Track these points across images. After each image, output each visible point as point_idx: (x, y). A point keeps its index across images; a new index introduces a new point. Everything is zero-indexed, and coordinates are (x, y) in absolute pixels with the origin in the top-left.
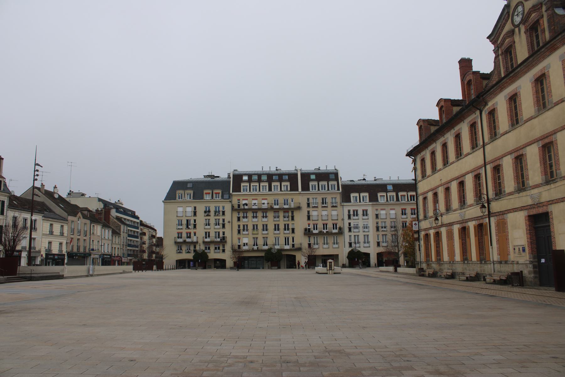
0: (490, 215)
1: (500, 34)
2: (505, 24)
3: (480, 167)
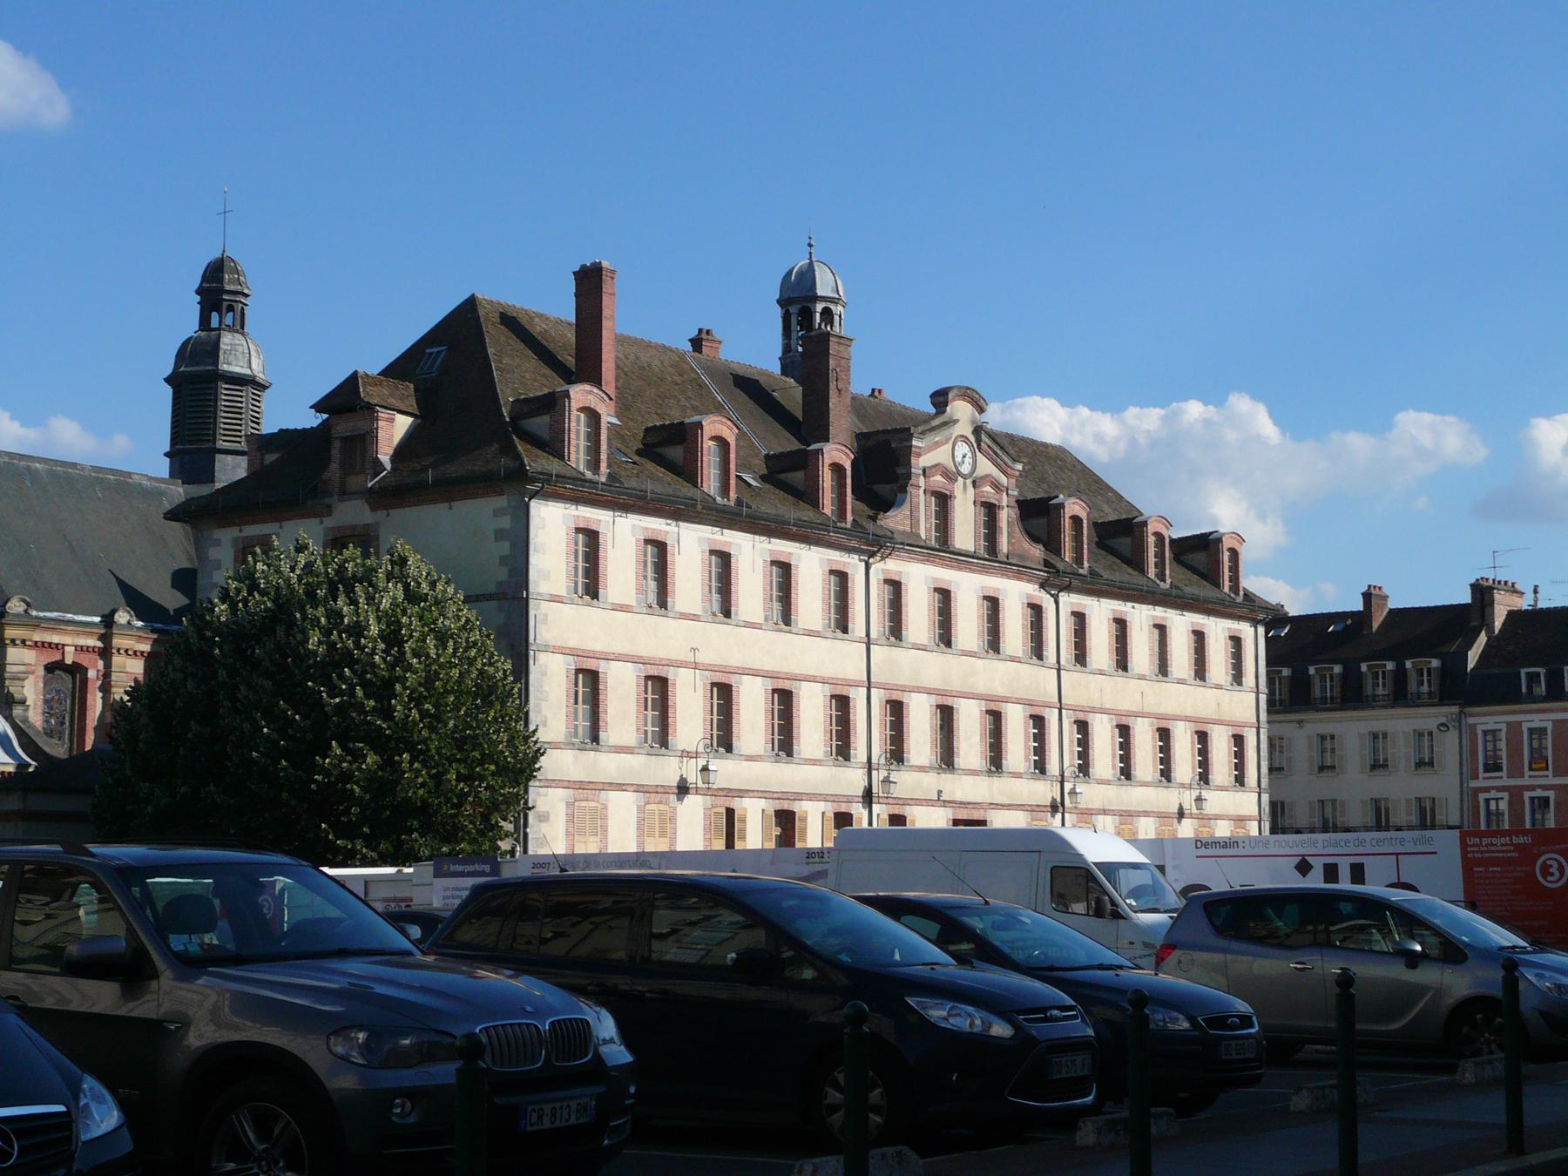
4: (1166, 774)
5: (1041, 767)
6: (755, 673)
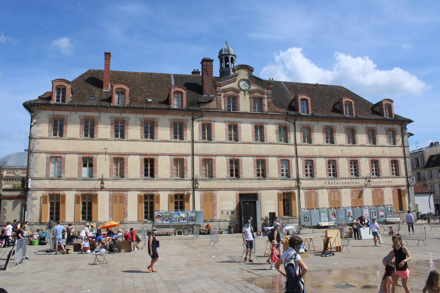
0: (194, 189)
1: (226, 84)
2: (232, 82)
3: (187, 155)
4: (357, 174)
5: (288, 176)
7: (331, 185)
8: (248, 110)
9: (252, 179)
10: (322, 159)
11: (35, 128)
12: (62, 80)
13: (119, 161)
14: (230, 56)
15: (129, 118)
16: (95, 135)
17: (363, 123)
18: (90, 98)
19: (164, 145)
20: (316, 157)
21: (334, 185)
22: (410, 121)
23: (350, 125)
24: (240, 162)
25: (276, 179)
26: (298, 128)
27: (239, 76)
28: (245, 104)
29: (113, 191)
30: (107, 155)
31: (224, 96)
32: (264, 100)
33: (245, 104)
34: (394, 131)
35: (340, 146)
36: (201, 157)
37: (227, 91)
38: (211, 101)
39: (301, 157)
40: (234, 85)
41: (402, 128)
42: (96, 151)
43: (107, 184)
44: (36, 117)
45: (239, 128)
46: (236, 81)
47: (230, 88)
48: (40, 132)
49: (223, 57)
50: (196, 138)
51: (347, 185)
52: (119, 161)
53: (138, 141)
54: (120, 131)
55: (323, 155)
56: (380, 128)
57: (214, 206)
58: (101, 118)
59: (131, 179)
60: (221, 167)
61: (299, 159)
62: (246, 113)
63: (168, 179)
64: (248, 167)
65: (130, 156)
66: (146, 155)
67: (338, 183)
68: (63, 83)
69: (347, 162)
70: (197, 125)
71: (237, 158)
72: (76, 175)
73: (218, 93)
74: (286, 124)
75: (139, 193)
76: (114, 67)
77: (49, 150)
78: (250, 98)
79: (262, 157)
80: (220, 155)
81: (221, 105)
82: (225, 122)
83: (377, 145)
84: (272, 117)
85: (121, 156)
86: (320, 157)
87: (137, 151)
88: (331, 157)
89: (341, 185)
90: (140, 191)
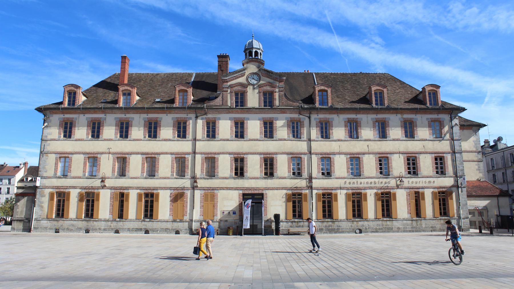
0: (194, 188)
1: (233, 80)
2: (240, 77)
3: (188, 154)
6: (137, 153)
7: (351, 186)
8: (257, 106)
9: (257, 178)
10: (343, 156)
11: (46, 131)
12: (72, 85)
13: (123, 161)
14: (254, 50)
15: (133, 118)
16: (100, 136)
17: (397, 113)
18: (106, 101)
19: (168, 144)
20: (334, 154)
21: (355, 185)
22: (464, 109)
23: (380, 116)
24: (245, 160)
25: (284, 178)
26: (314, 123)
27: (248, 70)
28: (253, 99)
29: (114, 189)
30: (110, 155)
31: (231, 92)
32: (275, 94)
33: (253, 99)
34: (440, 122)
35: (366, 140)
36: (203, 155)
37: (235, 87)
38: (216, 98)
39: (316, 154)
40: (242, 80)
41: (451, 118)
42: (101, 150)
43: (108, 183)
44: (48, 120)
45: (245, 125)
46: (244, 75)
47: (237, 83)
48: (50, 134)
49: (247, 52)
50: (199, 136)
51: (373, 185)
52: (123, 161)
53: (141, 140)
54: (124, 131)
55: (344, 151)
56: (421, 119)
57: (214, 206)
58: (107, 119)
59: (132, 178)
60: (225, 166)
61: (313, 156)
62: (254, 108)
63: (168, 178)
64: (254, 166)
65: (133, 156)
66: (148, 154)
67: (361, 183)
68: (73, 88)
69: (374, 159)
70: (200, 123)
71: (242, 156)
72: (81, 174)
73: (225, 89)
74: (300, 119)
75: (139, 191)
76: (131, 70)
77: (58, 151)
78: (259, 92)
79: (269, 154)
80: (223, 153)
81: (227, 101)
82: (230, 119)
83: (416, 138)
84: (283, 111)
85: (124, 156)
86: (340, 153)
87: (139, 151)
88: (353, 154)
89: (366, 186)
90: (140, 190)
